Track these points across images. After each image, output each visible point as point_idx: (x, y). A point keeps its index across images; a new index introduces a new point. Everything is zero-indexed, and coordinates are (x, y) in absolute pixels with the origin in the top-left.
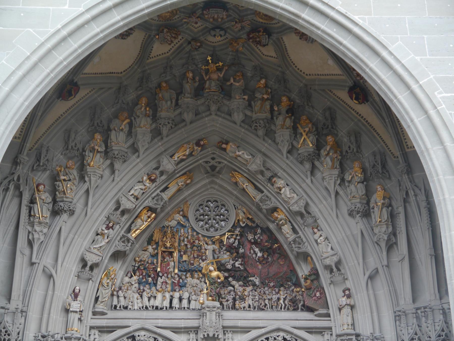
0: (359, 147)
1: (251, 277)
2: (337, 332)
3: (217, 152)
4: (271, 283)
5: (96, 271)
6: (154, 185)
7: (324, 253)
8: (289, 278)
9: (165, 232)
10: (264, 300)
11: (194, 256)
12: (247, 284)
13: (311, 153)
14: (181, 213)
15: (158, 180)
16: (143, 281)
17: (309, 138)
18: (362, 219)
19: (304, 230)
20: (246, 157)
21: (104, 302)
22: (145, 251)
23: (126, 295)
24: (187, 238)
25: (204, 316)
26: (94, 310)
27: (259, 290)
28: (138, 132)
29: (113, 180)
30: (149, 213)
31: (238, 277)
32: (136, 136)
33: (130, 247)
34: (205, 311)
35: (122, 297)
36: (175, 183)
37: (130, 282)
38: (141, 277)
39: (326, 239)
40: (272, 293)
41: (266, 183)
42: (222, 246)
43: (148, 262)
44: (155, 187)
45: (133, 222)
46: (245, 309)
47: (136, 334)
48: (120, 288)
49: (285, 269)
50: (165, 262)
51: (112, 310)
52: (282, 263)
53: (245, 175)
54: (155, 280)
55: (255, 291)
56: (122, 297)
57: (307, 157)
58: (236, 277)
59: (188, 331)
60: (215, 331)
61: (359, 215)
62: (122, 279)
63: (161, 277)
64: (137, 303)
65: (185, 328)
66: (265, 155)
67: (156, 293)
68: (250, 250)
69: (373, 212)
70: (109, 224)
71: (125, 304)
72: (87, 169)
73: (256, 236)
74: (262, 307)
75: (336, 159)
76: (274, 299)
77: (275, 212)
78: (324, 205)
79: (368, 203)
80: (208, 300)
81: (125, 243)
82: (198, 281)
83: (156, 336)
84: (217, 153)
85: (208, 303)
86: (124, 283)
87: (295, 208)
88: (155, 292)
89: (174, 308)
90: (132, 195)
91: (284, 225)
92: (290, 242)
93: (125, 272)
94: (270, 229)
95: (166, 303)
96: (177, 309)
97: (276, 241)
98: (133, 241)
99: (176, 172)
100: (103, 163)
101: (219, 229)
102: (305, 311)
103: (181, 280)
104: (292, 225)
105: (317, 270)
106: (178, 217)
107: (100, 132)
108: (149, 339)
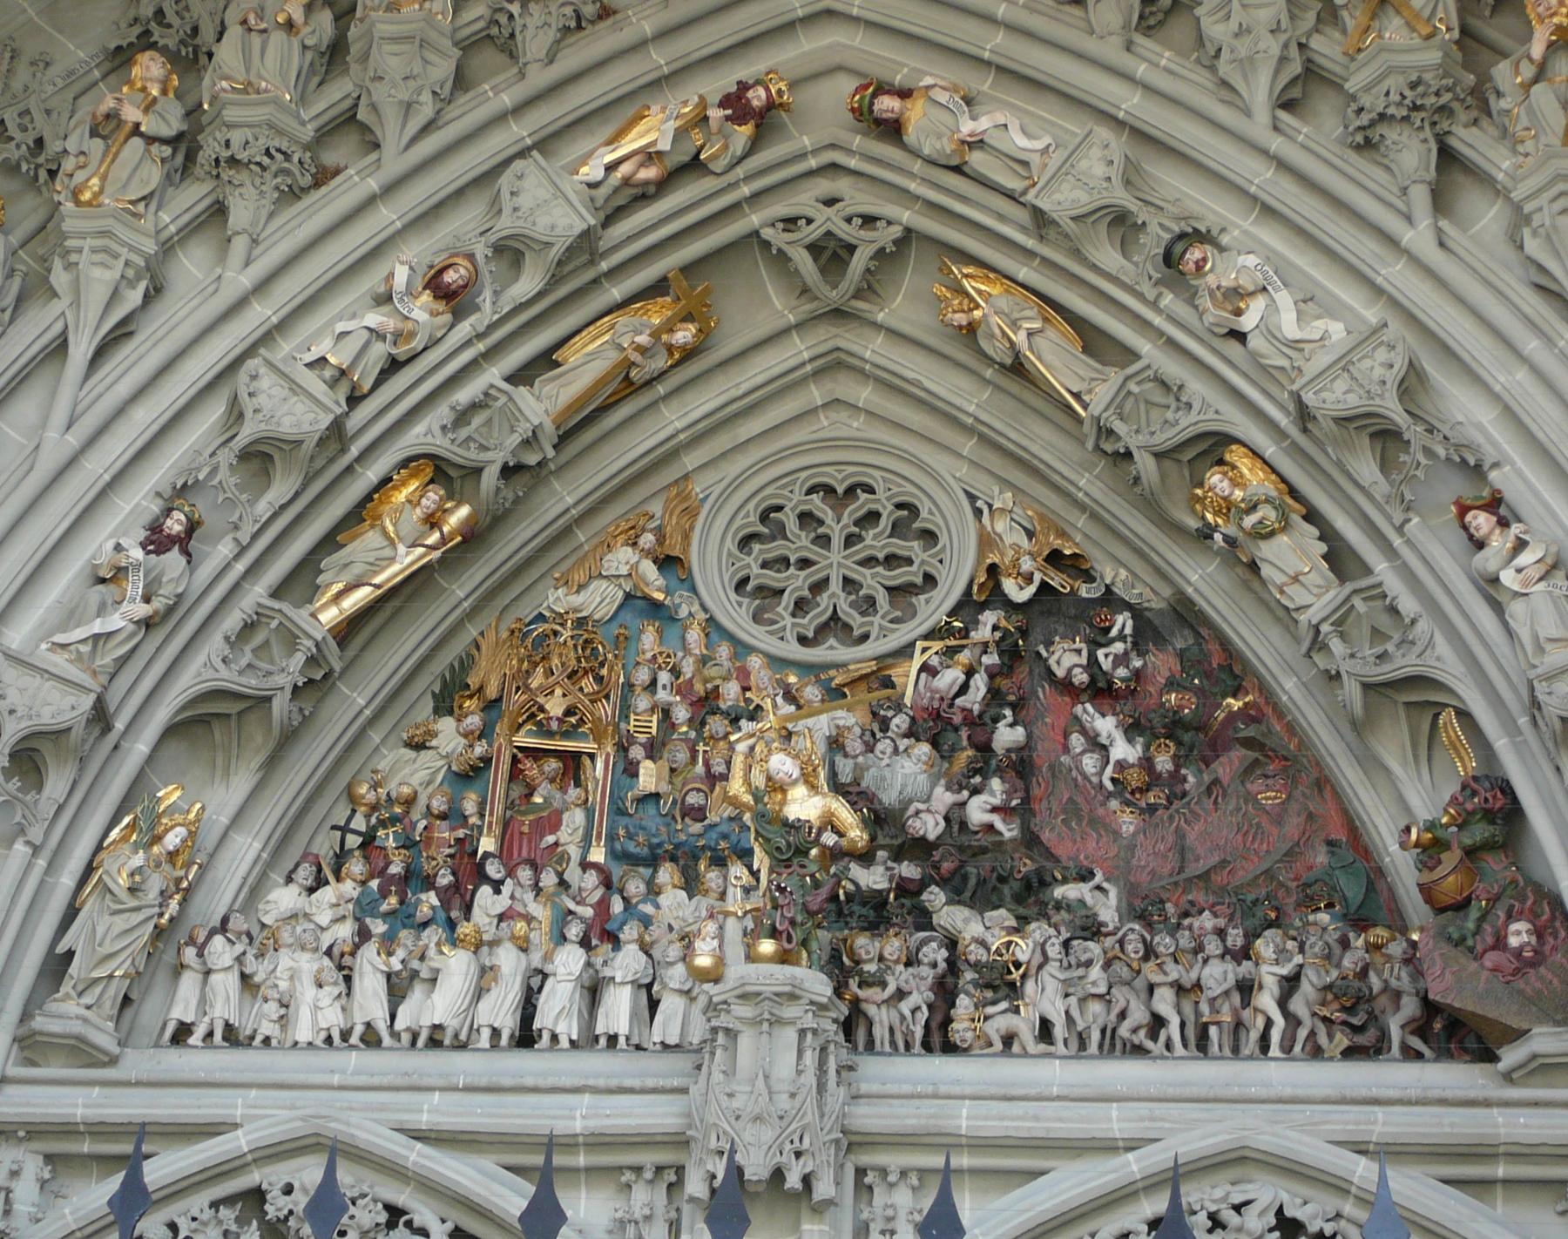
1: (1065, 881)
4: (1201, 912)
6: (465, 329)
7: (1548, 647)
13: (1427, 76)
14: (648, 540)
15: (487, 296)
19: (1409, 542)
20: (1022, 141)
22: (419, 746)
24: (676, 672)
25: (719, 1052)
29: (216, 291)
30: (433, 497)
34: (723, 1021)
36: (599, 342)
38: (374, 884)
39: (1555, 566)
44: (467, 344)
45: (329, 542)
46: (1016, 1048)
52: (1269, 798)
53: (1024, 273)
54: (457, 902)
58: (972, 882)
62: (255, 890)
63: (497, 886)
68: (1066, 736)
73: (1100, 653)
74: (1135, 1031)
76: (1211, 983)
84: (853, 163)
87: (1336, 397)
89: (546, 1036)
91: (1272, 534)
96: (564, 1043)
98: (317, 645)
99: (604, 266)
102: (1437, 1059)
105: (1507, 789)
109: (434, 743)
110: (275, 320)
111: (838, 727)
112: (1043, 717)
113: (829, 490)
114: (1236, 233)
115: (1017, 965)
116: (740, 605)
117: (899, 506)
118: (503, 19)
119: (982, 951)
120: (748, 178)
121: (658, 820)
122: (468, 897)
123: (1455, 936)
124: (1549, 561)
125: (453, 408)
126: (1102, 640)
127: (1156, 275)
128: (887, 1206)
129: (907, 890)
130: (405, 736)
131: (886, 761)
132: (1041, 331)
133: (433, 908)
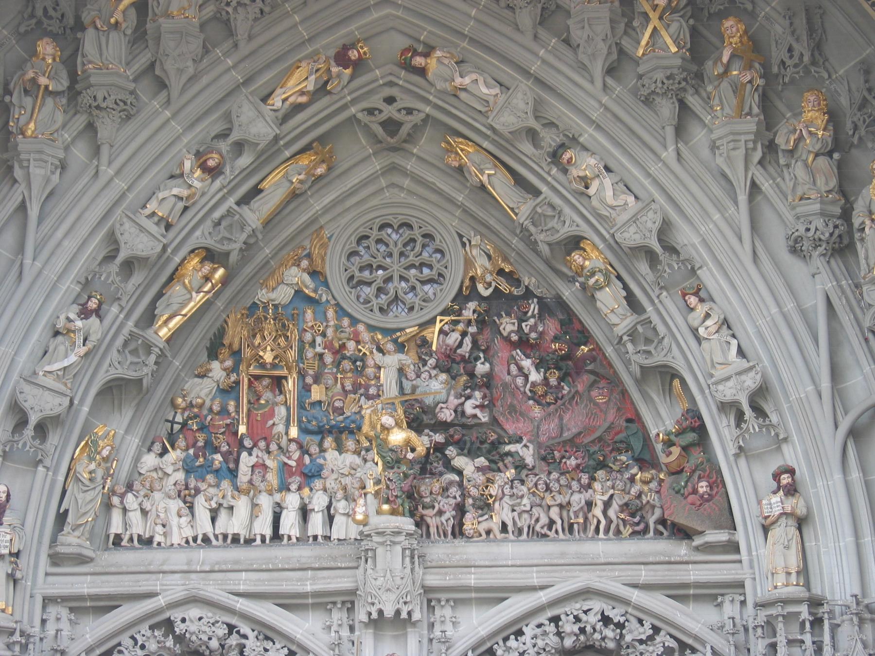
0: (818, 48)
1: (510, 443)
2: (759, 595)
3: (400, 79)
4: (569, 458)
5: (54, 439)
6: (218, 183)
7: (718, 366)
8: (621, 442)
9: (259, 321)
10: (546, 508)
11: (343, 387)
12: (500, 464)
13: (675, 71)
14: (305, 263)
16: (197, 464)
17: (667, 27)
18: (828, 262)
19: (660, 301)
20: (485, 90)
21: (82, 529)
22: (202, 376)
23: (147, 505)
24: (324, 335)
25: (369, 560)
26: (52, 552)
27: (531, 480)
28: (162, 30)
31: (472, 443)
32: (158, 39)
33: (155, 367)
35: (135, 510)
37: (160, 468)
38: (191, 451)
39: (723, 324)
40: (571, 488)
41: (544, 165)
42: (426, 354)
43: (211, 410)
44: (220, 190)
45: (160, 295)
46: (491, 536)
47: (176, 615)
48: (130, 487)
49: (611, 415)
50: (263, 406)
51: (107, 549)
53: (485, 144)
55: (522, 482)
56: (135, 510)
57: (663, 83)
59: (327, 603)
60: (401, 601)
61: (820, 250)
62: (137, 460)
64: (180, 527)
65: (316, 594)
66: (539, 81)
67: (233, 498)
69: (862, 240)
70: (87, 302)
71: (145, 533)
72: (17, 145)
73: (523, 325)
75: (749, 86)
76: (574, 504)
77: (577, 252)
78: (716, 225)
79: (846, 214)
80: (379, 512)
81: (139, 357)
82: (358, 460)
83: (234, 621)
84: (401, 83)
85: (377, 521)
86: (142, 471)
87: (631, 237)
88: (229, 494)
90: (154, 214)
91: (601, 288)
92: (621, 338)
93: (144, 440)
94: (564, 302)
95: (264, 527)
97: (585, 336)
98: (161, 350)
99: (282, 143)
100: (64, 126)
101: (416, 308)
102: (669, 538)
103: (307, 458)
104: (626, 287)
105: (700, 418)
106: (296, 276)
107: (54, 36)
108: (213, 629)
109: (210, 375)
110: (126, 188)
111: (403, 365)
112: (497, 353)
113: (390, 225)
114: (586, 136)
115: (491, 496)
116: (351, 293)
117: (425, 236)
118: (224, 13)
119: (476, 490)
120: (349, 94)
121: (321, 413)
122: (235, 454)
123: (676, 489)
124: (720, 322)
125: (213, 221)
126: (525, 318)
127: (549, 160)
128: (441, 617)
129: (439, 448)
130: (196, 372)
131: (427, 383)
132: (495, 174)
133: (220, 463)
